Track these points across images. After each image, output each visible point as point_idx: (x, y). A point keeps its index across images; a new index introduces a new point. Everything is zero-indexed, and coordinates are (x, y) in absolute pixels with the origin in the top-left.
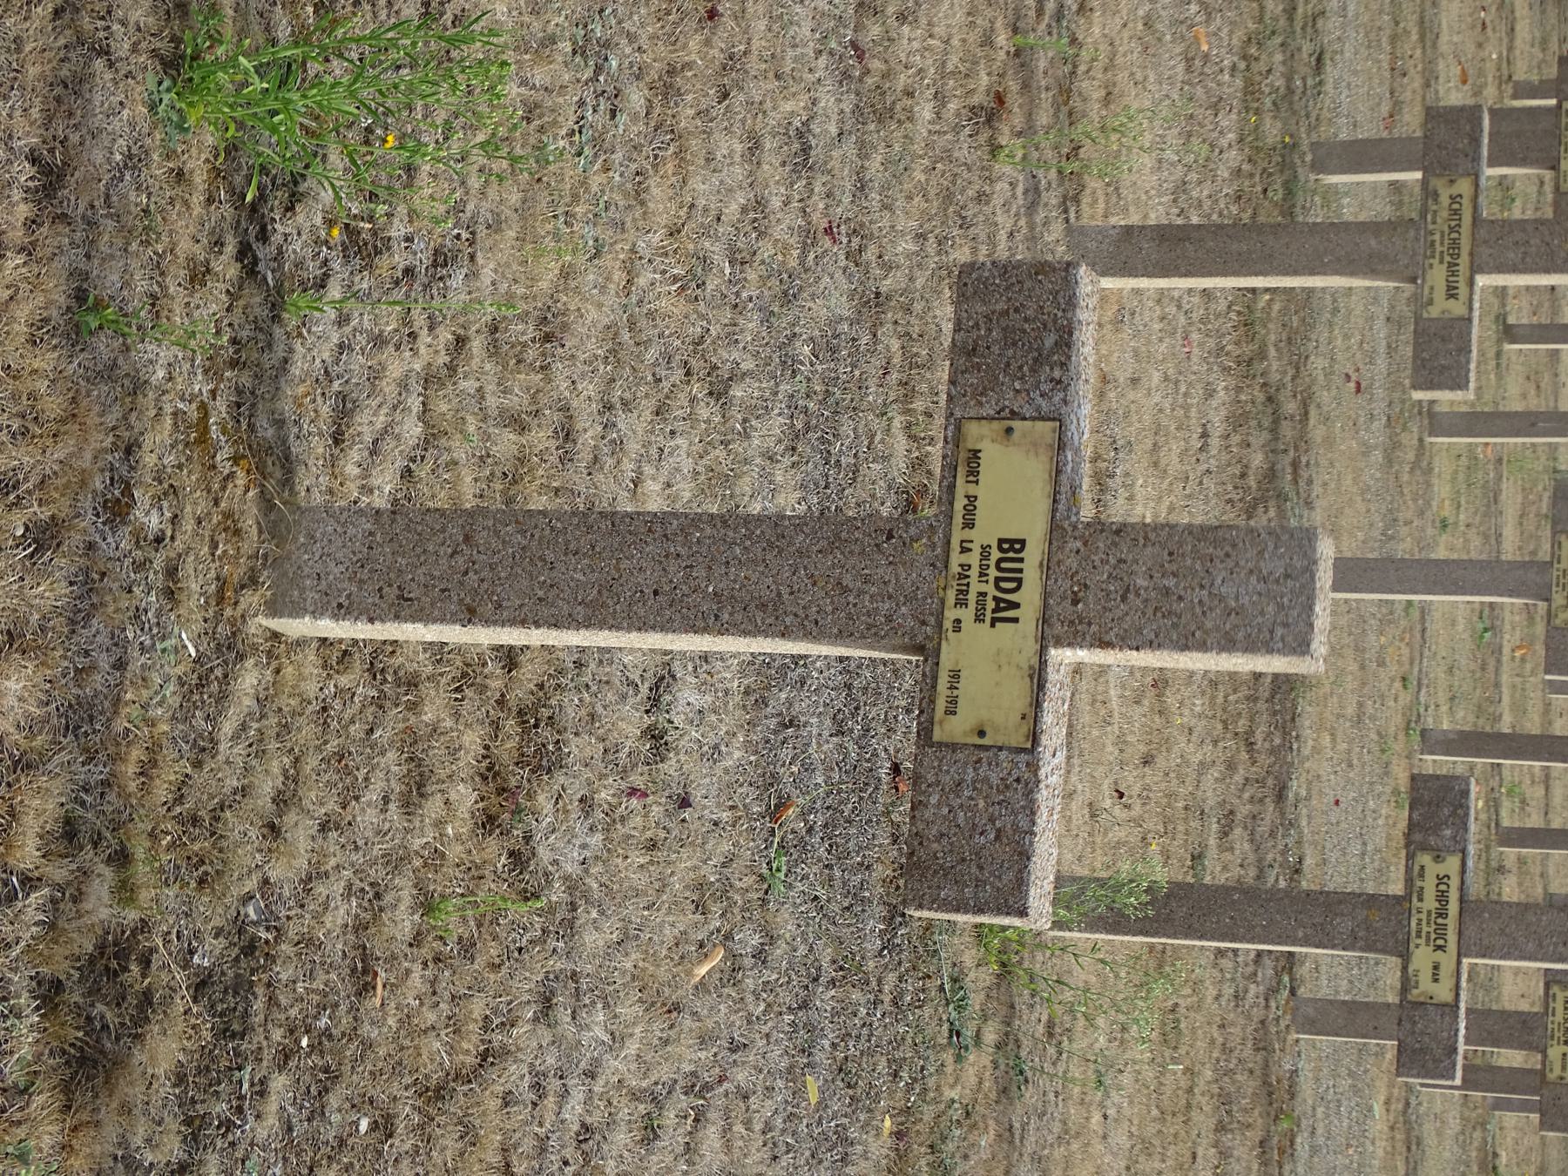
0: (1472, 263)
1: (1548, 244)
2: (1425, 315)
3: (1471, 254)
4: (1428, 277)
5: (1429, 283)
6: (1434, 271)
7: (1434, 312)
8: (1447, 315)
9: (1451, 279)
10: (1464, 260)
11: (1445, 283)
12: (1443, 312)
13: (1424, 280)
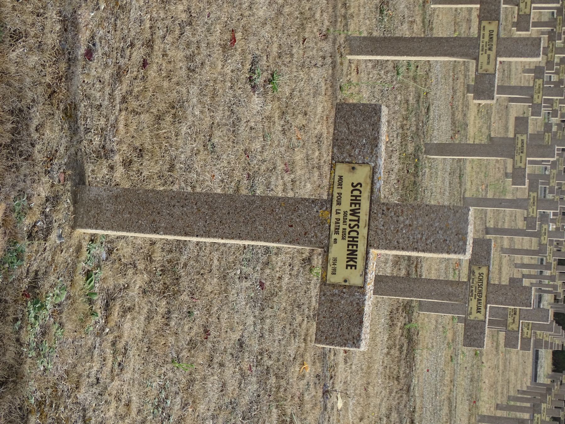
0: (486, 300)
1: (514, 295)
2: (469, 318)
3: (486, 296)
4: (470, 304)
5: (470, 306)
6: (472, 301)
7: (472, 317)
8: (477, 319)
9: (478, 305)
10: (483, 299)
11: (476, 307)
12: (475, 318)
13: (468, 305)
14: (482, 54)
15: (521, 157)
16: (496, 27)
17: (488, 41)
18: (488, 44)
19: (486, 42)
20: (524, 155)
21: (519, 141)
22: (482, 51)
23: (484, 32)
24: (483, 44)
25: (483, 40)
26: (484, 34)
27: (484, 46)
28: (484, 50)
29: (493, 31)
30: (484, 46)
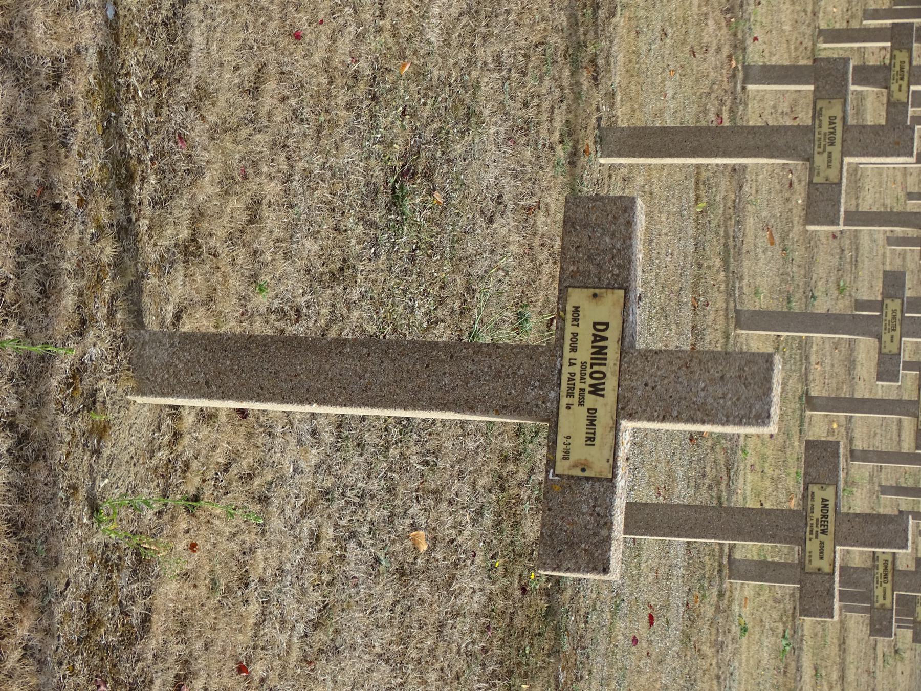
14: (569, 407)
15: (822, 543)
16: (618, 311)
17: (589, 362)
18: (589, 371)
19: (583, 364)
20: (828, 540)
21: (815, 503)
22: (570, 395)
23: (575, 329)
24: (571, 369)
25: (572, 355)
26: (575, 335)
27: (577, 377)
28: (576, 392)
29: (607, 324)
30: (577, 377)
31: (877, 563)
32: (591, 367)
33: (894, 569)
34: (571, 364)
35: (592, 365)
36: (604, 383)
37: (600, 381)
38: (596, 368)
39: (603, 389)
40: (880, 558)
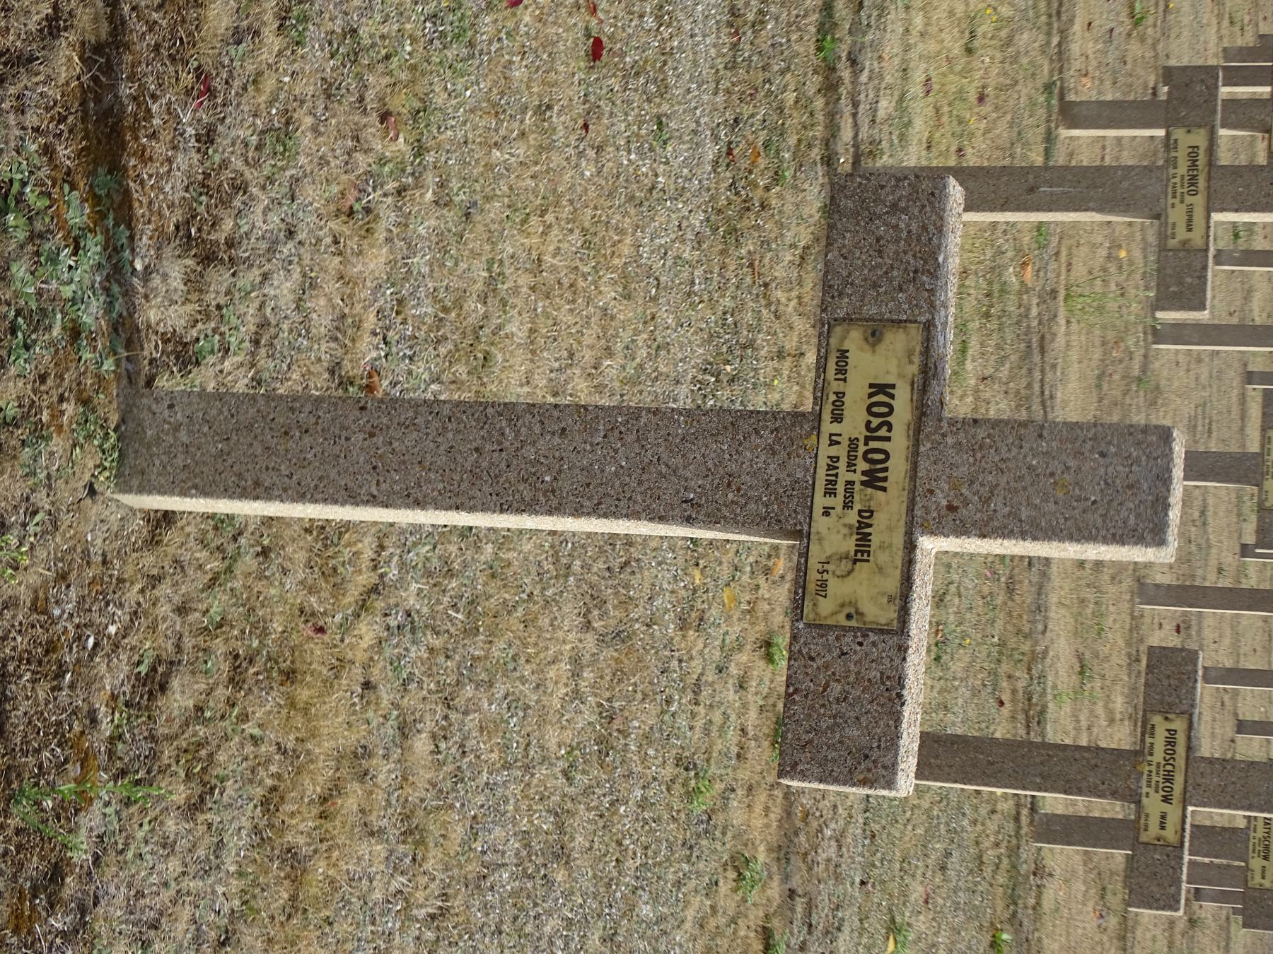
31: (1174, 154)
32: (866, 444)
33: (1211, 163)
34: (833, 443)
35: (867, 440)
36: (886, 470)
37: (879, 466)
38: (873, 445)
39: (885, 479)
40: (1179, 142)
